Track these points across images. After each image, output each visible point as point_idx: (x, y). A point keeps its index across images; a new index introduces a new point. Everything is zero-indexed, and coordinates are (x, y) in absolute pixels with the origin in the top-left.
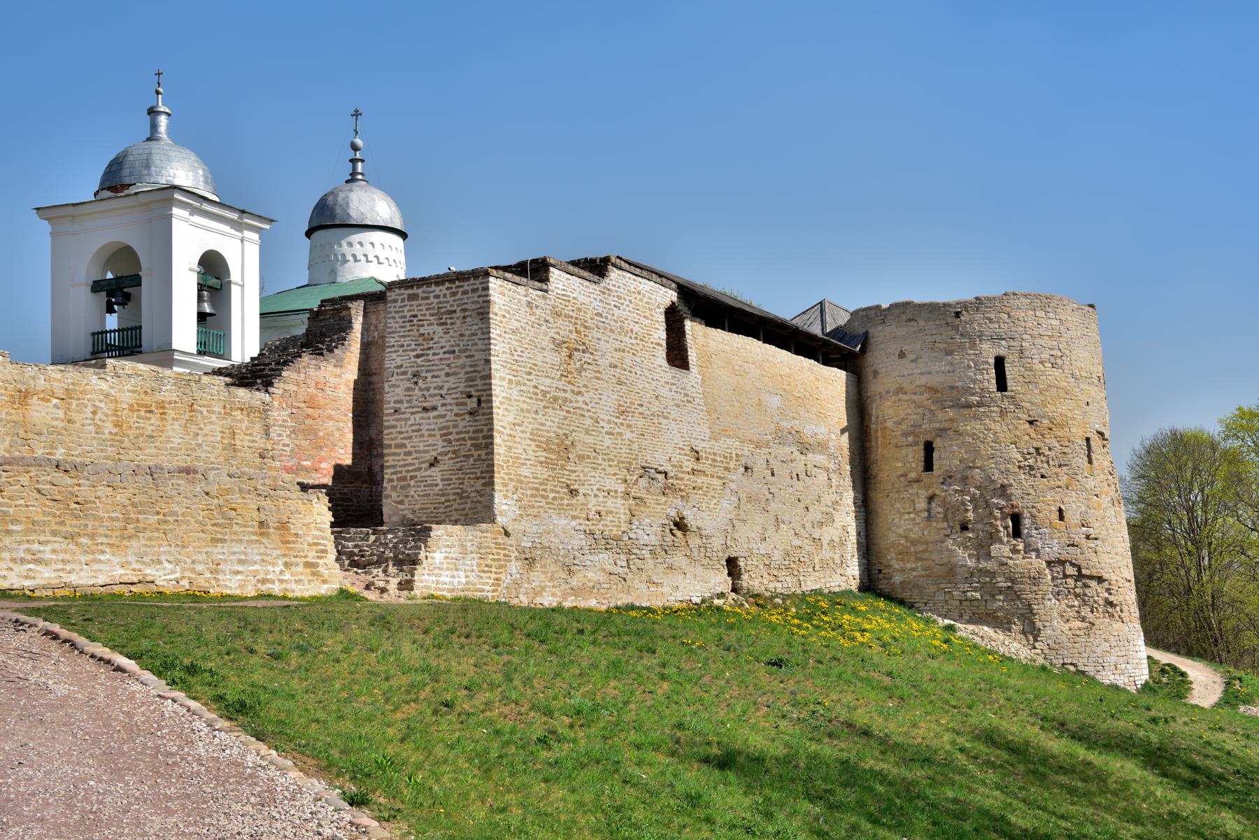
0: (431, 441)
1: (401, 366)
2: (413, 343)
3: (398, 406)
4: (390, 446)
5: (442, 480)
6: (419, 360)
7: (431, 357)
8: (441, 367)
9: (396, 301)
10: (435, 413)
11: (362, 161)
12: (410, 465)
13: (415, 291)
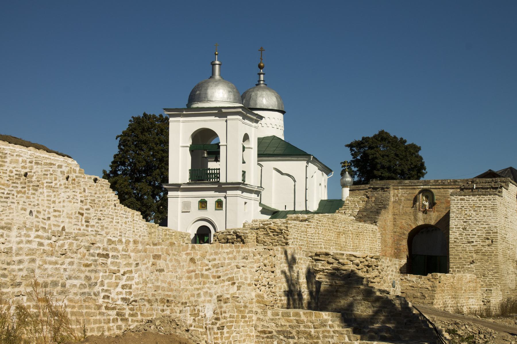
0: (470, 255)
1: (457, 225)
2: (463, 217)
3: (455, 240)
4: (452, 255)
5: (476, 269)
6: (465, 224)
7: (470, 223)
8: (475, 227)
9: (454, 200)
10: (472, 244)
11: (264, 74)
12: (461, 263)
13: (463, 197)
